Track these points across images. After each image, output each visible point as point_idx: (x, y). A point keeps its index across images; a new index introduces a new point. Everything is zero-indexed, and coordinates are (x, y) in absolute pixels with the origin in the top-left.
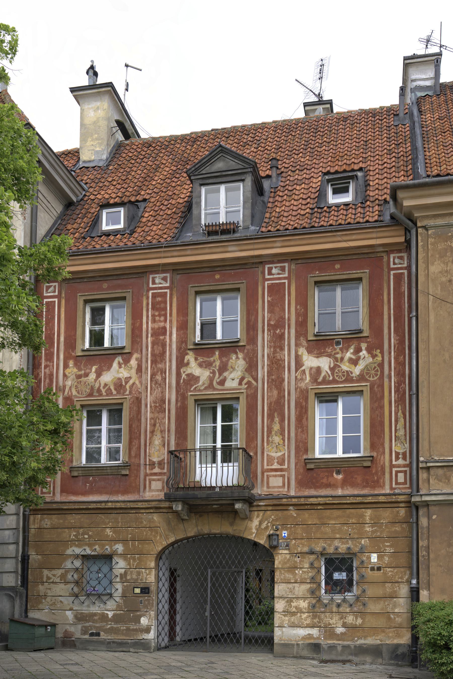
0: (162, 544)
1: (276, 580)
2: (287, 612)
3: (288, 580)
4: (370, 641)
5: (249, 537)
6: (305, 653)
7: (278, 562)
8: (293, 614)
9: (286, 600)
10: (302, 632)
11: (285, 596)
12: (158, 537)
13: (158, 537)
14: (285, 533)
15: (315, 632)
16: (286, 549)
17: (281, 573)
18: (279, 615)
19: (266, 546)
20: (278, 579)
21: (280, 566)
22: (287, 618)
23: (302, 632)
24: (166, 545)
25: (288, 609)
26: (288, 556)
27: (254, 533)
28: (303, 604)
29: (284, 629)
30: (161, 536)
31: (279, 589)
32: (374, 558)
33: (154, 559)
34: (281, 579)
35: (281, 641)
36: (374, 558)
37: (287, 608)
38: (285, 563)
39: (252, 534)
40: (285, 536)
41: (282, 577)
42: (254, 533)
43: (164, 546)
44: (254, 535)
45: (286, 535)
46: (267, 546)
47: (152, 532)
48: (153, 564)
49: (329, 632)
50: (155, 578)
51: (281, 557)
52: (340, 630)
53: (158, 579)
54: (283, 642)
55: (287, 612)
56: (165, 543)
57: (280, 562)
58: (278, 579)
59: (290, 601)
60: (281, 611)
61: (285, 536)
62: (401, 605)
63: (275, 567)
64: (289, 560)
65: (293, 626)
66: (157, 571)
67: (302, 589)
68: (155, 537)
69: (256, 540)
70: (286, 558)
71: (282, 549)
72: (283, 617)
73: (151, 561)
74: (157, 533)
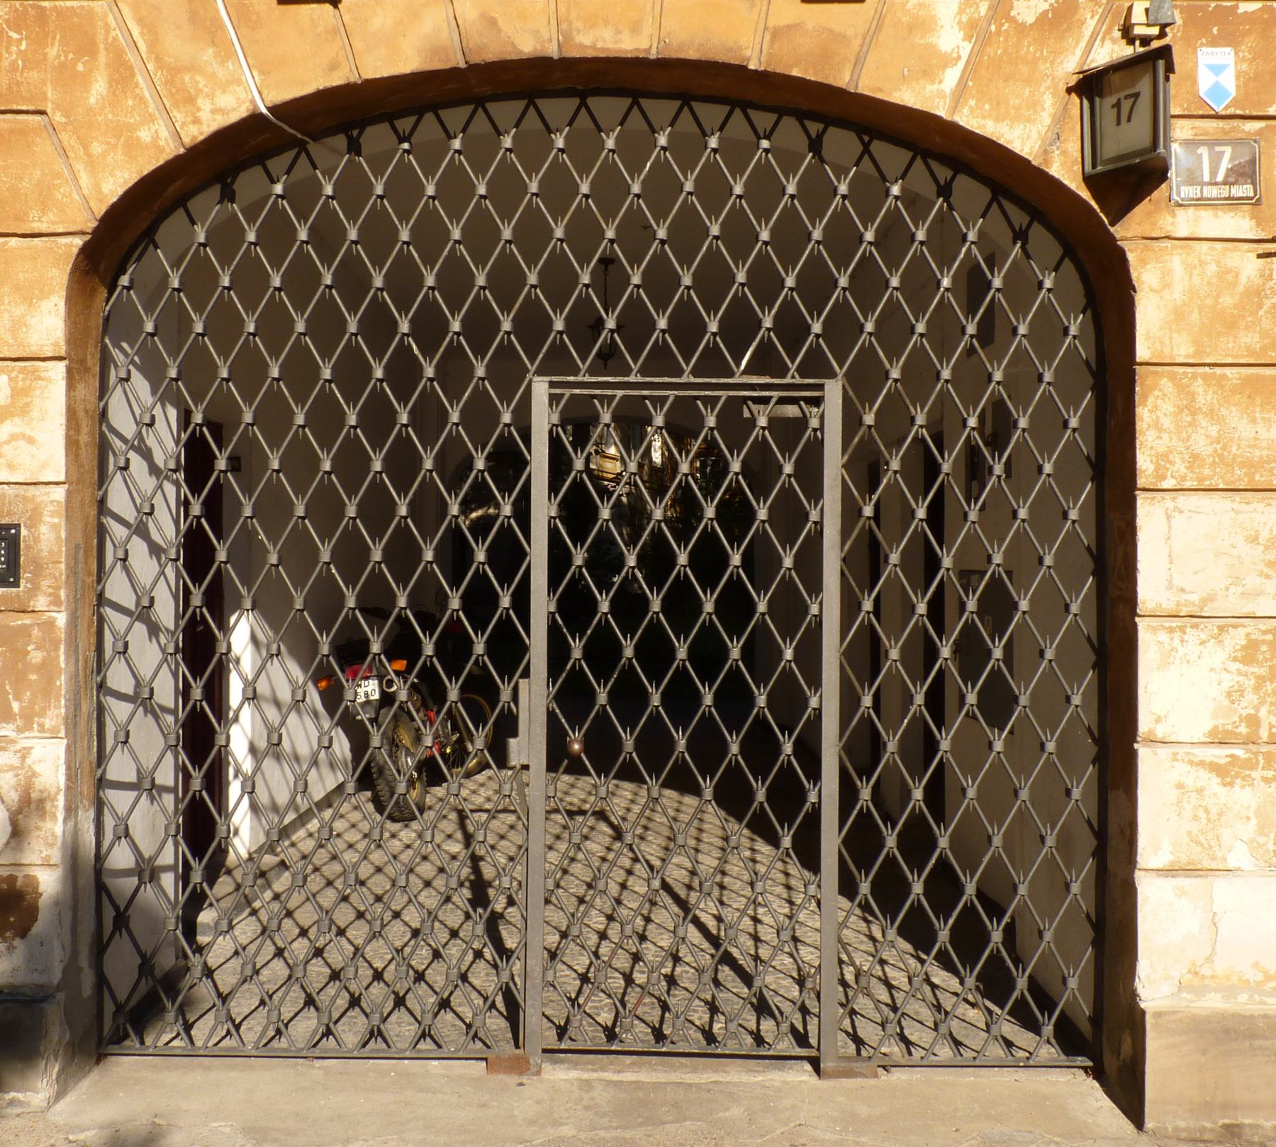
0: (132, 147)
1: (1144, 462)
3: (1250, 465)
5: (907, 97)
9: (1237, 638)
11: (1231, 604)
12: (99, 86)
13: (99, 86)
16: (1233, 202)
17: (1189, 406)
18: (1181, 772)
19: (1056, 170)
20: (1163, 458)
21: (1183, 351)
22: (1244, 797)
24: (171, 150)
25: (1253, 721)
26: (1248, 265)
27: (948, 61)
29: (1222, 889)
30: (122, 77)
33: (59, 276)
34: (1195, 460)
35: (1200, 991)
37: (1246, 705)
38: (1230, 323)
39: (931, 64)
40: (1217, 89)
41: (1201, 444)
42: (948, 61)
43: (149, 164)
44: (951, 77)
45: (1229, 82)
46: (1066, 168)
47: (39, 42)
48: (49, 323)
50: (72, 444)
53: (95, 454)
54: (1214, 1003)
56: (160, 140)
57: (1179, 315)
58: (1163, 458)
60: (1199, 731)
61: (1217, 89)
63: (1143, 351)
64: (1255, 295)
66: (86, 391)
68: (67, 76)
69: (969, 119)
70: (1226, 277)
71: (1201, 203)
72: (1212, 782)
73: (30, 295)
74: (88, 49)
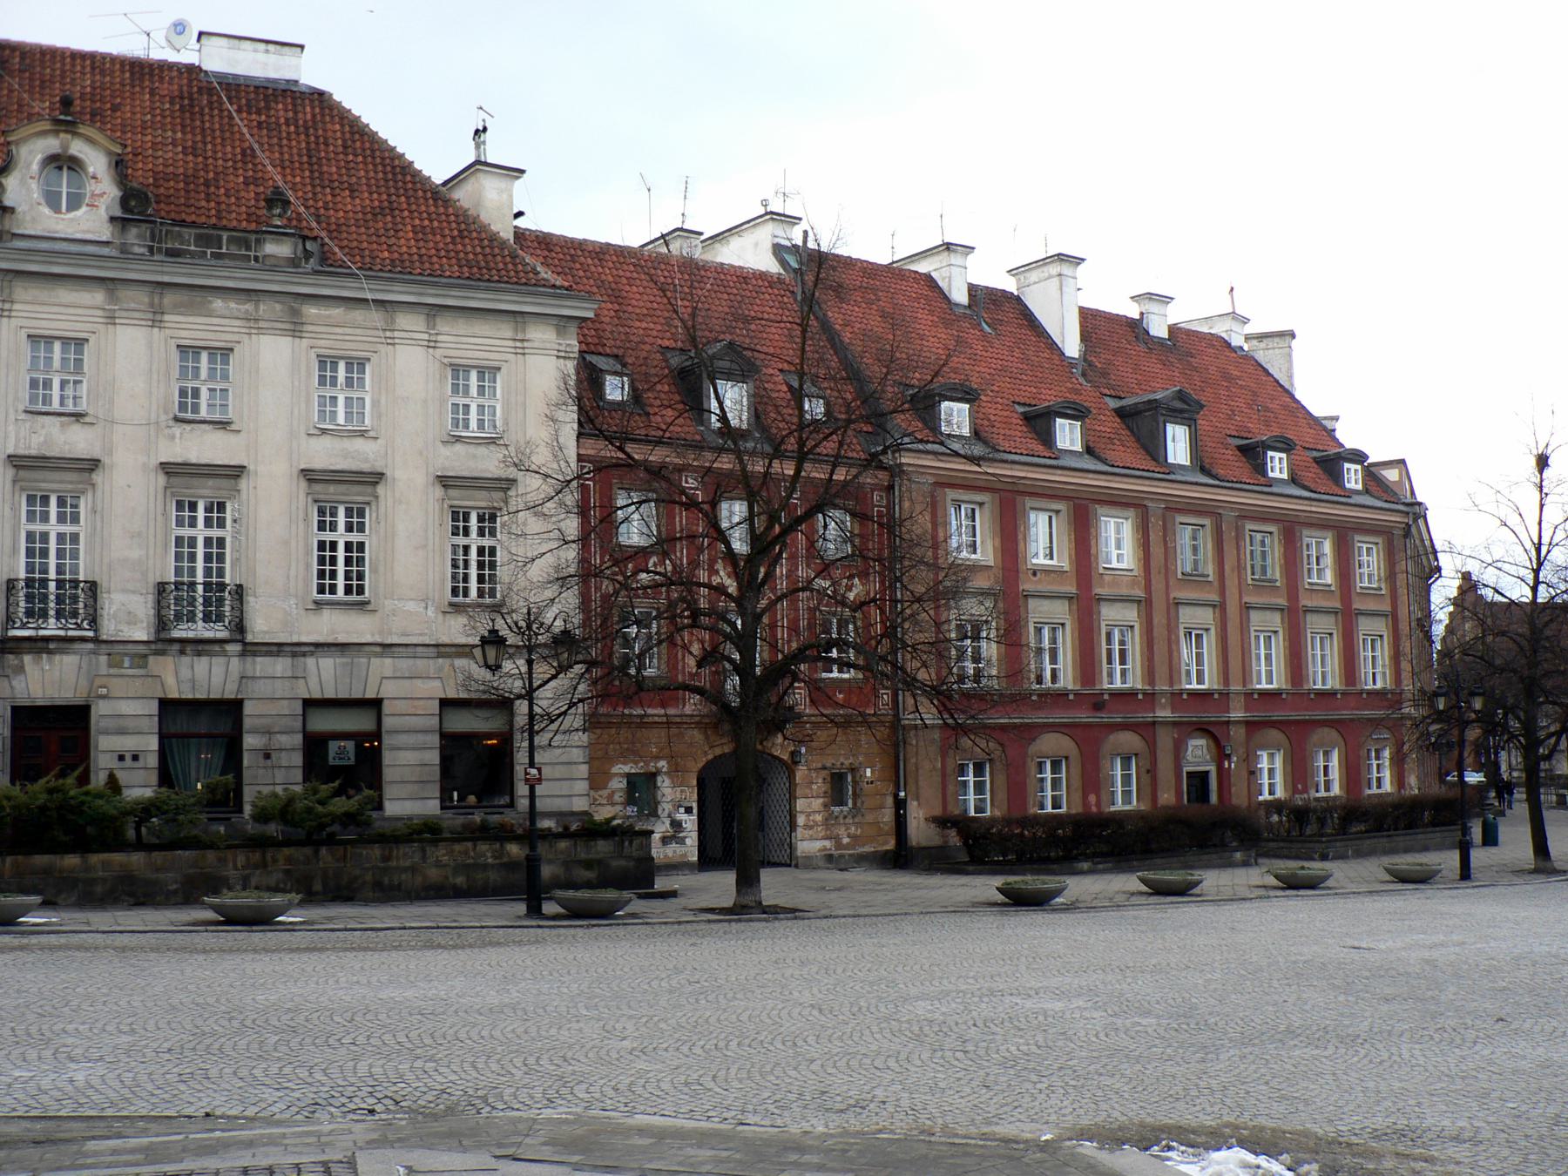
2: (807, 827)
4: (868, 849)
6: (821, 863)
7: (799, 775)
8: (811, 828)
10: (818, 845)
14: (803, 750)
15: (827, 844)
23: (818, 845)
28: (819, 818)
31: (800, 804)
32: (869, 772)
36: (869, 772)
49: (839, 845)
51: (801, 773)
52: (846, 840)
55: (807, 827)
59: (808, 815)
62: (887, 816)
65: (811, 839)
67: (817, 803)
